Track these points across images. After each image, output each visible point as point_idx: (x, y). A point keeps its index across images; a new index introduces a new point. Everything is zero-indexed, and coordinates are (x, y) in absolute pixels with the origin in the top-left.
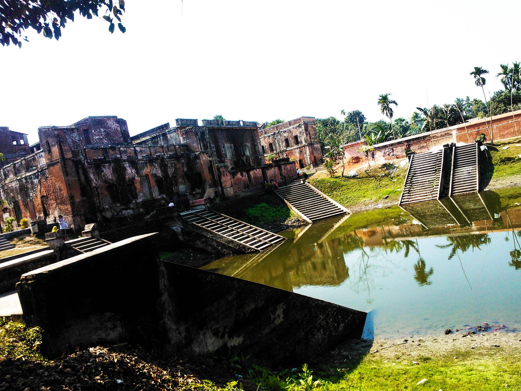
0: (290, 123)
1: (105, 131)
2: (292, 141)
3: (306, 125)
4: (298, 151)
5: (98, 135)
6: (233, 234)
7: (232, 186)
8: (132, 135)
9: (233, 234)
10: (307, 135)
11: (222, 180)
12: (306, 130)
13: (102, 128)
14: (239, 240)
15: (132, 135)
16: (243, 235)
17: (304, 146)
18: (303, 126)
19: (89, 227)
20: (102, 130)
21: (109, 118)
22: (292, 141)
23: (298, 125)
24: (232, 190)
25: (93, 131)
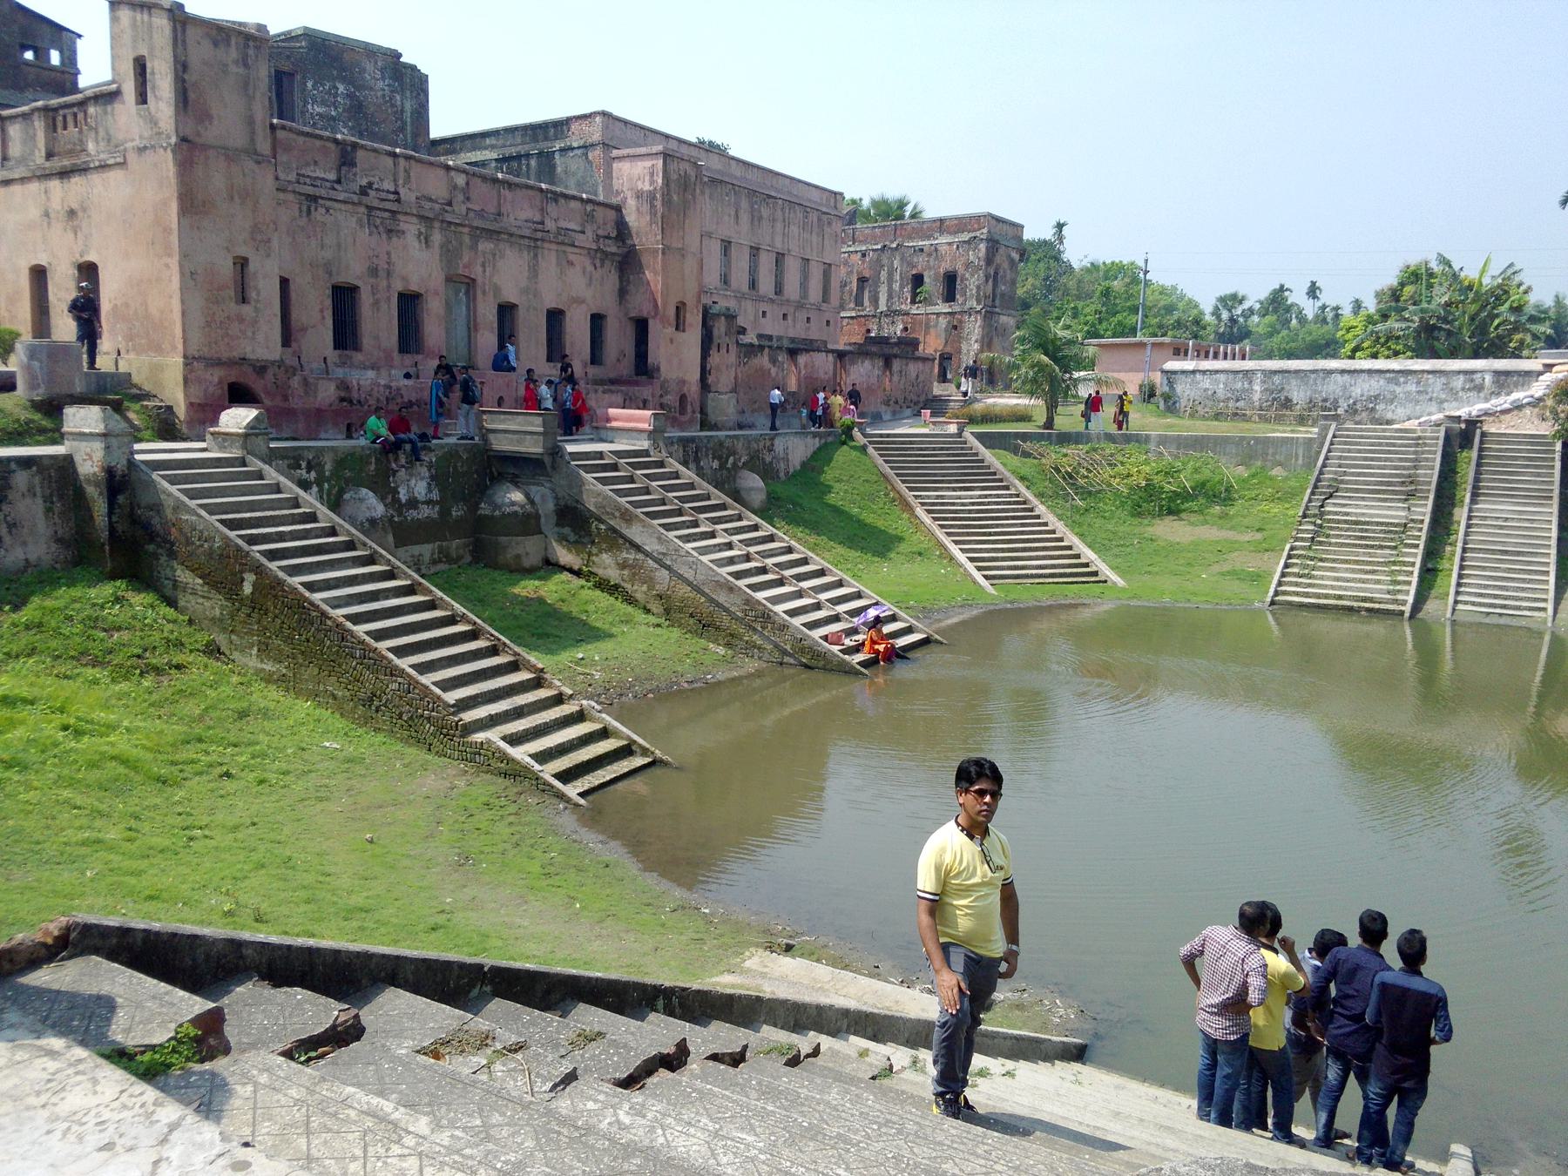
0: (941, 224)
1: (350, 96)
2: (931, 285)
3: (993, 244)
4: (943, 322)
5: (323, 103)
6: (731, 561)
7: (734, 390)
8: (437, 130)
9: (731, 561)
10: (987, 278)
11: (710, 359)
12: (989, 260)
13: (344, 80)
14: (753, 587)
15: (437, 130)
16: (763, 570)
17: (970, 312)
18: (983, 246)
19: (237, 418)
20: (341, 88)
21: (371, 51)
22: (931, 285)
23: (965, 237)
24: (734, 401)
25: (310, 85)
